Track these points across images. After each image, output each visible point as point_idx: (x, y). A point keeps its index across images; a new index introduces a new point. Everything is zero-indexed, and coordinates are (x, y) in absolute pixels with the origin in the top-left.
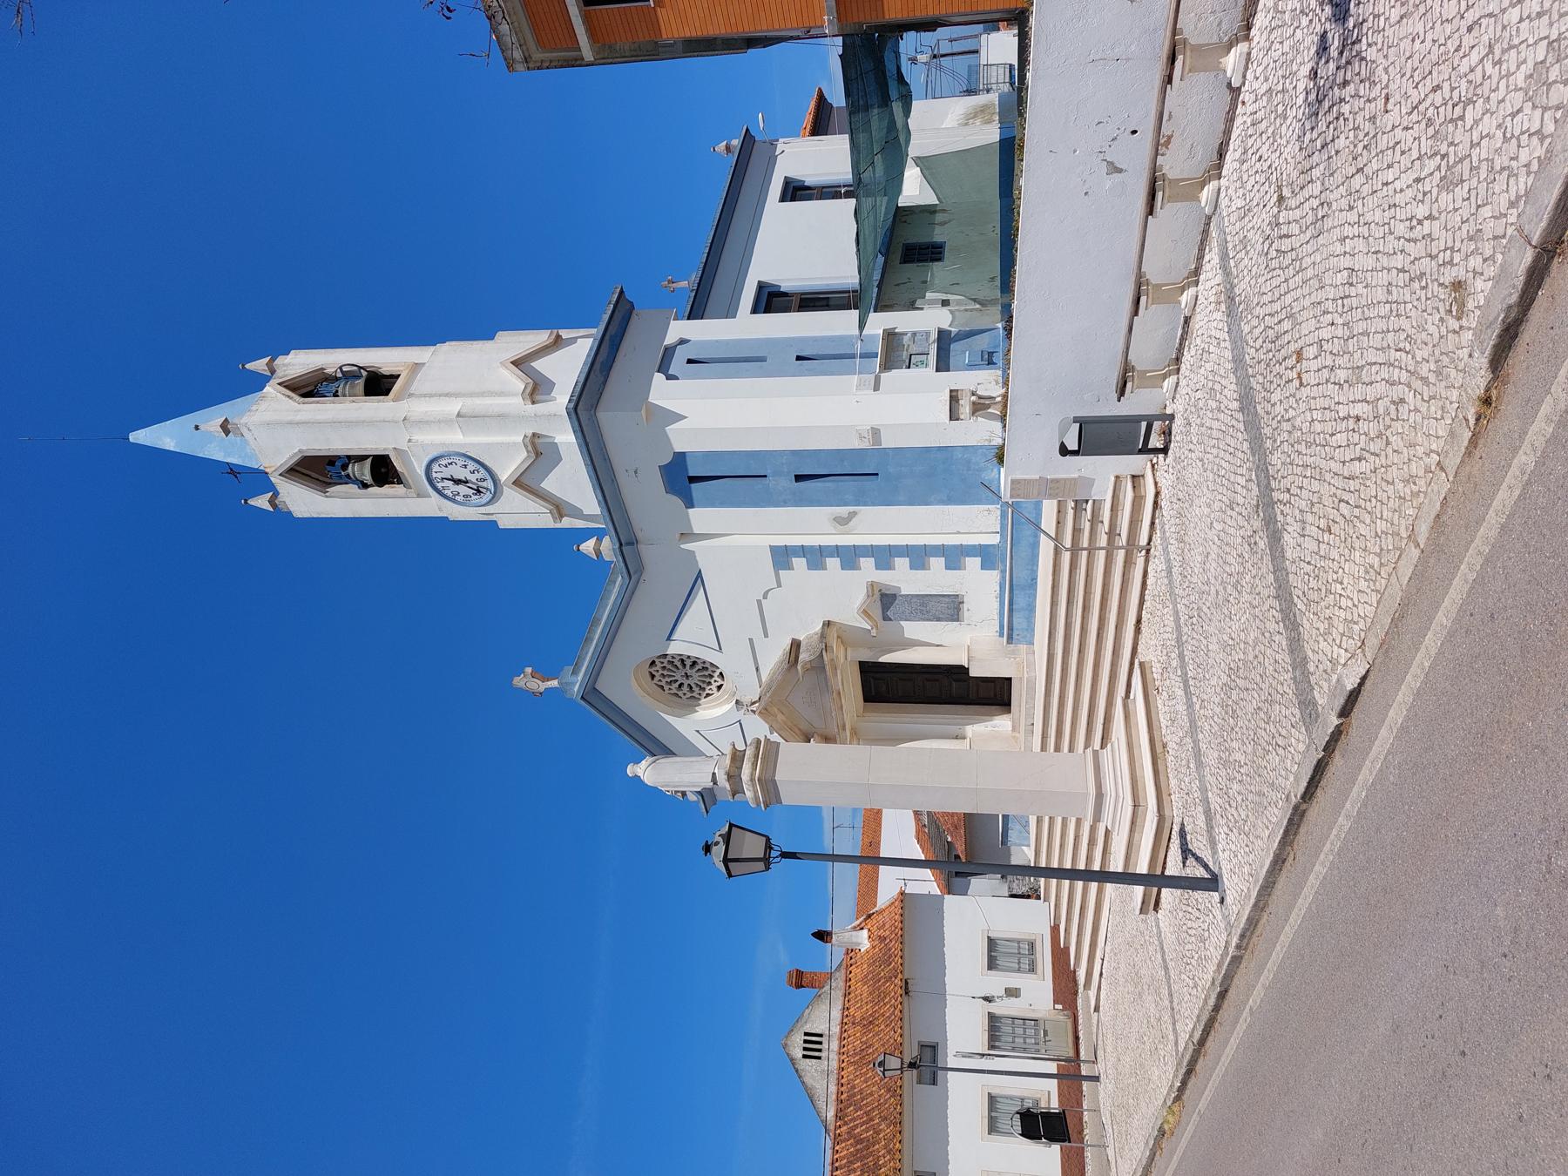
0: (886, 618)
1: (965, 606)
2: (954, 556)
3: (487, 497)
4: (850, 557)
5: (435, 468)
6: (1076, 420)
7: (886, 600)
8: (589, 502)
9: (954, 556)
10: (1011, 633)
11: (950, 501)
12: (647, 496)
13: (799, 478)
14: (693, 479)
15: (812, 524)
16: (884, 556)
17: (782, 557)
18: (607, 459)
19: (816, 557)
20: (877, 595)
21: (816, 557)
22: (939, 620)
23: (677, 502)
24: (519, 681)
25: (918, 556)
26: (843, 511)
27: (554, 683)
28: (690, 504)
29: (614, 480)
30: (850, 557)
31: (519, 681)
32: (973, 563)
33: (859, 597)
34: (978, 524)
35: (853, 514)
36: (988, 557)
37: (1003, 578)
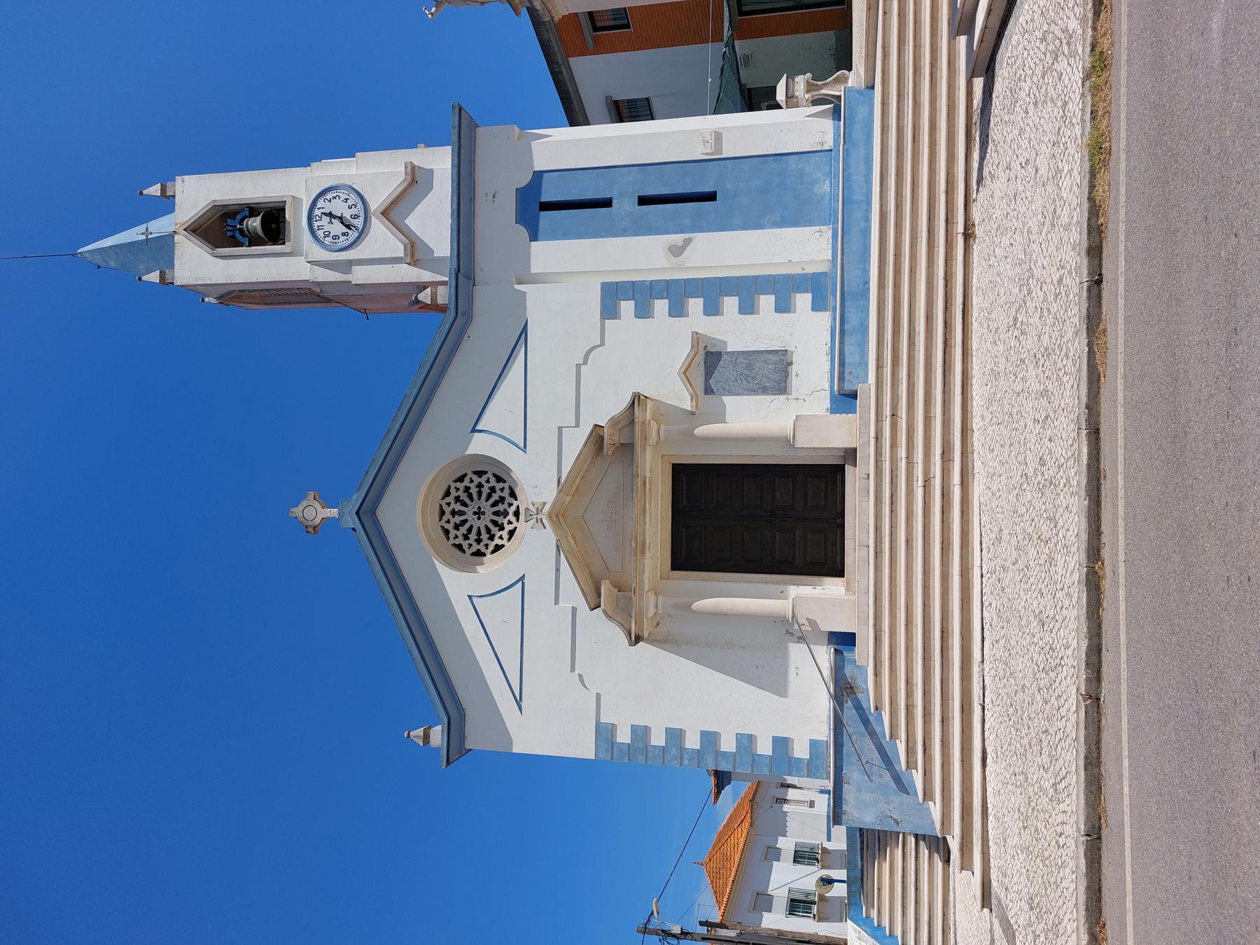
0: (708, 391)
1: (794, 369)
3: (353, 235)
4: (677, 294)
5: (320, 203)
7: (711, 366)
8: (442, 246)
9: (783, 289)
10: (845, 399)
11: (784, 223)
12: (496, 214)
13: (644, 201)
14: (546, 206)
15: (644, 254)
16: (712, 292)
20: (702, 353)
22: (764, 391)
23: (522, 231)
24: (297, 511)
25: (746, 290)
26: (678, 238)
27: (333, 512)
28: (534, 237)
29: (472, 199)
30: (677, 294)
31: (297, 511)
32: (803, 300)
33: (683, 350)
34: (806, 247)
35: (688, 242)
36: (815, 285)
37: (834, 319)
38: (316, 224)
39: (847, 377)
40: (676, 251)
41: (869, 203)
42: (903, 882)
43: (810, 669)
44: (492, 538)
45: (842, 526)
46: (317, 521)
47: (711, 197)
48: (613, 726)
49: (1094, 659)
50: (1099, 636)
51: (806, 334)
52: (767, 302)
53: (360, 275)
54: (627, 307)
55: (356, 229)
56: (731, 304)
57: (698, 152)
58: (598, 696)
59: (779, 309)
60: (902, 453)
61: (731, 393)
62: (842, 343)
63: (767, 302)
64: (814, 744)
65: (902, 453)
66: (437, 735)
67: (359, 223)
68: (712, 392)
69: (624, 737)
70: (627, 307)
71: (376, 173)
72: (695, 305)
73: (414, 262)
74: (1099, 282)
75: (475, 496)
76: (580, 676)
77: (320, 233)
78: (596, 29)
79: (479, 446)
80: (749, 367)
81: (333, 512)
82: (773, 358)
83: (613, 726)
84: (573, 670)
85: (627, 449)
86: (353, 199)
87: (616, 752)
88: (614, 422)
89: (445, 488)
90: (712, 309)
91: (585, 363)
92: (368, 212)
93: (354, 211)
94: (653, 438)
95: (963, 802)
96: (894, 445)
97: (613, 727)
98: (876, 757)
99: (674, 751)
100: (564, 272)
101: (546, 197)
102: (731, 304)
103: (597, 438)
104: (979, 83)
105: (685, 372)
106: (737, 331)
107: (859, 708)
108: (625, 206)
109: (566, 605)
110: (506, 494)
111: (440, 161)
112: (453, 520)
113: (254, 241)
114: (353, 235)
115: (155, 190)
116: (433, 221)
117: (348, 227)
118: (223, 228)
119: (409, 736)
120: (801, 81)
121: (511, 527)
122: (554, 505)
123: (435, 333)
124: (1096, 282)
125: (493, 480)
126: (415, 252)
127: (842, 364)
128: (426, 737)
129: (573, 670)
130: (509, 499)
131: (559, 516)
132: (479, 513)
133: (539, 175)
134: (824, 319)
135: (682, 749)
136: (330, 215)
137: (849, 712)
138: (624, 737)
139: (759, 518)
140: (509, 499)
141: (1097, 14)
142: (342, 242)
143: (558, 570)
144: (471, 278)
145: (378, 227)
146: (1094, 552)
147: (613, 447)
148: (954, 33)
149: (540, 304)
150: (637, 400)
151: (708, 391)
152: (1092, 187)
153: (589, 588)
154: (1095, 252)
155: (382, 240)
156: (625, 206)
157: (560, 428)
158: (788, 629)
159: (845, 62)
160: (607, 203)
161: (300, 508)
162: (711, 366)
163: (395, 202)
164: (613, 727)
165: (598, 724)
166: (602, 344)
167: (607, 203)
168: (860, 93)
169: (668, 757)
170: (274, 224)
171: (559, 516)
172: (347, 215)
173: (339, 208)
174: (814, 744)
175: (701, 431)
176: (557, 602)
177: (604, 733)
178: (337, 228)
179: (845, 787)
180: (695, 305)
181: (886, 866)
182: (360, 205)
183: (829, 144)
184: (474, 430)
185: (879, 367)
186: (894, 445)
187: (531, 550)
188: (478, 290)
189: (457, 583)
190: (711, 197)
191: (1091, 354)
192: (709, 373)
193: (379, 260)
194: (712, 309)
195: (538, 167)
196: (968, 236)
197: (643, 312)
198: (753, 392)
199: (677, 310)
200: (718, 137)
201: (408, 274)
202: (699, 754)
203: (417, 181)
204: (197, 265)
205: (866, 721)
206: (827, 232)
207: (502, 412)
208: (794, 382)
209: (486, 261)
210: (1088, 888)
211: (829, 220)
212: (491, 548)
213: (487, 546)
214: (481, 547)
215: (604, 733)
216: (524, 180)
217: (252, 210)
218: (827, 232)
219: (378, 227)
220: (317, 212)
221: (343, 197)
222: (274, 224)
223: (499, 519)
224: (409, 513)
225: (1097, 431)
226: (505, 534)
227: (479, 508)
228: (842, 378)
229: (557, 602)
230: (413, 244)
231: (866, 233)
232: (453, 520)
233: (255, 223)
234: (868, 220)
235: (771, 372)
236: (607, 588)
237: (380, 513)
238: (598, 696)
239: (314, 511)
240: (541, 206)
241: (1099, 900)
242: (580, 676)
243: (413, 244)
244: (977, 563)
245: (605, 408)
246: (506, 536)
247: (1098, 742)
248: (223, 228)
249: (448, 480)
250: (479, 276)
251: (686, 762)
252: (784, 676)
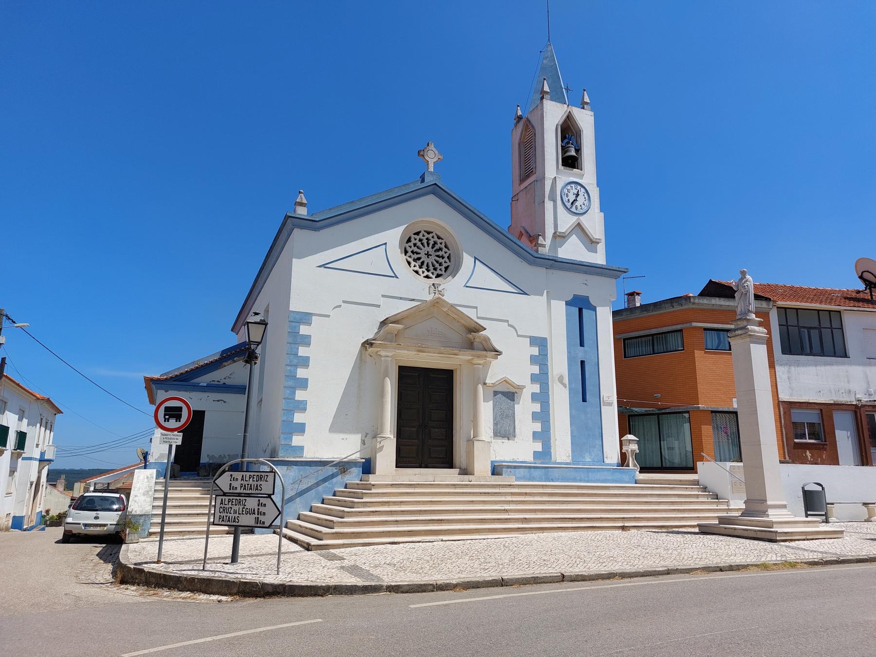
1: (506, 441)
2: (544, 436)
3: (569, 205)
4: (542, 378)
6: (823, 489)
7: (508, 395)
9: (544, 436)
11: (573, 436)
12: (578, 285)
13: (582, 363)
14: (580, 310)
15: (560, 364)
16: (543, 398)
17: (540, 343)
18: (597, 274)
19: (541, 359)
20: (514, 390)
21: (541, 359)
22: (496, 424)
25: (543, 416)
26: (566, 380)
27: (431, 169)
28: (568, 303)
29: (586, 273)
30: (542, 378)
31: (432, 147)
32: (538, 447)
33: (517, 380)
34: (562, 451)
35: (565, 386)
36: (545, 454)
38: (573, 185)
39: (509, 470)
40: (561, 380)
41: (588, 481)
42: (197, 506)
43: (346, 447)
44: (415, 260)
45: (420, 467)
46: (427, 158)
47: (584, 400)
48: (310, 324)
49: (580, 578)
50: (590, 580)
51: (521, 449)
52: (538, 427)
53: (549, 205)
54: (535, 351)
55: (571, 207)
56: (537, 407)
57: (604, 393)
58: (328, 316)
59: (534, 433)
60: (509, 498)
61: (494, 406)
62: (525, 467)
63: (538, 427)
64: (301, 448)
65: (509, 498)
66: (302, 212)
67: (573, 209)
68: (495, 395)
69: (304, 330)
70: (535, 351)
71: (595, 222)
72: (536, 388)
73: (555, 235)
74: (721, 570)
75: (437, 254)
76: (340, 306)
77: (569, 187)
78: (624, 340)
79: (467, 260)
80: (507, 416)
81: (431, 169)
82: (512, 431)
83: (310, 324)
84: (344, 302)
85: (470, 346)
86: (585, 208)
87: (294, 324)
88: (487, 339)
89: (442, 236)
90: (535, 397)
91: (509, 325)
92: (576, 215)
93: (579, 207)
94: (476, 361)
95: (361, 533)
96: (512, 494)
97: (309, 323)
98: (304, 486)
99: (295, 361)
100: (550, 317)
101: (585, 312)
102: (537, 407)
103: (477, 329)
104: (697, 530)
105: (506, 381)
106: (525, 409)
107: (333, 476)
108: (581, 353)
109: (382, 301)
110: (439, 272)
111: (599, 258)
112: (424, 238)
113: (564, 149)
114: (569, 205)
115: (587, 99)
116: (573, 250)
117: (572, 203)
118: (569, 132)
119: (300, 193)
120: (634, 447)
121: (421, 272)
122: (444, 301)
123: (522, 242)
124: (721, 570)
125: (446, 265)
126: (560, 238)
127: (515, 467)
128: (301, 204)
129: (344, 302)
130: (436, 273)
131: (438, 303)
132: (428, 255)
133: (594, 309)
134: (530, 458)
135: (296, 366)
136: (577, 195)
137: (330, 470)
138: (304, 330)
139: (428, 417)
140: (436, 273)
141: (805, 563)
142: (565, 199)
143: (413, 300)
144: (551, 267)
145: (573, 219)
146: (623, 575)
147: (472, 338)
148: (720, 518)
149: (537, 302)
150: (498, 353)
151: (496, 393)
152: (752, 565)
153: (398, 317)
154: (731, 568)
155: (566, 222)
156: (581, 353)
157: (476, 308)
158: (373, 435)
159: (643, 470)
160: (582, 344)
161: (434, 149)
162: (508, 395)
163: (583, 230)
164: (309, 323)
165: (310, 315)
166: (518, 336)
167: (582, 344)
168: (634, 477)
169: (292, 357)
170: (571, 162)
171: (438, 303)
172: (577, 204)
173: (581, 199)
174: (301, 448)
175: (480, 387)
176: (383, 296)
177: (306, 318)
178: (572, 198)
179: (285, 468)
180: (536, 388)
181: (198, 495)
182: (582, 211)
183: (607, 461)
184: (475, 258)
185: (543, 486)
186: (512, 494)
187: (415, 287)
188: (543, 270)
189: (394, 236)
190: (584, 400)
191: (697, 569)
192: (504, 394)
193: (557, 218)
194: (535, 397)
195: (598, 309)
196: (623, 528)
197: (533, 360)
198: (495, 419)
199: (534, 378)
200: (610, 404)
201: (549, 231)
202: (293, 377)
203: (591, 243)
204: (553, 114)
205: (325, 480)
206: (569, 460)
207: (485, 276)
208: (499, 441)
209: (558, 275)
210: (479, 582)
211: (574, 461)
212: (409, 259)
213: (410, 257)
214: (410, 254)
215: (306, 318)
216: (593, 302)
217: (578, 150)
218: (569, 460)
219: (573, 219)
220: (579, 187)
221: (586, 203)
222: (571, 162)
223: (425, 266)
224: (431, 213)
225: (668, 574)
226: (417, 268)
227: (431, 254)
228: (509, 467)
229: (383, 296)
230: (564, 237)
231: (575, 480)
232: (424, 238)
233: (573, 153)
234: (581, 481)
235: (505, 430)
236: (391, 329)
237: (431, 196)
238: (328, 316)
239: (432, 157)
240: (581, 306)
241: (473, 588)
242: (340, 306)
243: (564, 237)
244: (489, 537)
245: (493, 333)
246: (416, 269)
247: (545, 582)
248: (569, 132)
249: (446, 238)
250: (550, 271)
251: (289, 368)
252: (342, 431)
